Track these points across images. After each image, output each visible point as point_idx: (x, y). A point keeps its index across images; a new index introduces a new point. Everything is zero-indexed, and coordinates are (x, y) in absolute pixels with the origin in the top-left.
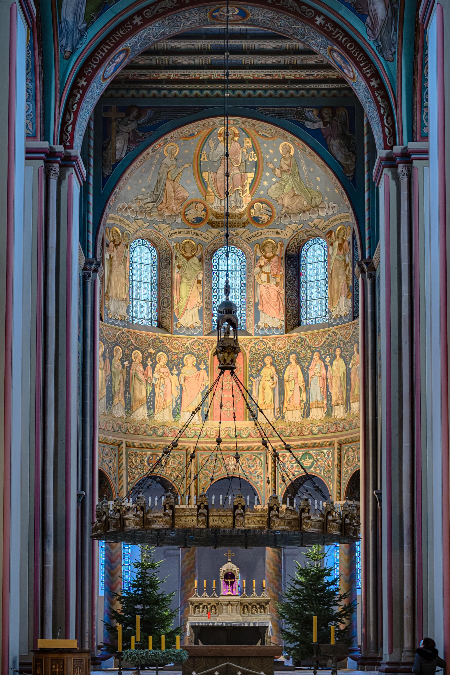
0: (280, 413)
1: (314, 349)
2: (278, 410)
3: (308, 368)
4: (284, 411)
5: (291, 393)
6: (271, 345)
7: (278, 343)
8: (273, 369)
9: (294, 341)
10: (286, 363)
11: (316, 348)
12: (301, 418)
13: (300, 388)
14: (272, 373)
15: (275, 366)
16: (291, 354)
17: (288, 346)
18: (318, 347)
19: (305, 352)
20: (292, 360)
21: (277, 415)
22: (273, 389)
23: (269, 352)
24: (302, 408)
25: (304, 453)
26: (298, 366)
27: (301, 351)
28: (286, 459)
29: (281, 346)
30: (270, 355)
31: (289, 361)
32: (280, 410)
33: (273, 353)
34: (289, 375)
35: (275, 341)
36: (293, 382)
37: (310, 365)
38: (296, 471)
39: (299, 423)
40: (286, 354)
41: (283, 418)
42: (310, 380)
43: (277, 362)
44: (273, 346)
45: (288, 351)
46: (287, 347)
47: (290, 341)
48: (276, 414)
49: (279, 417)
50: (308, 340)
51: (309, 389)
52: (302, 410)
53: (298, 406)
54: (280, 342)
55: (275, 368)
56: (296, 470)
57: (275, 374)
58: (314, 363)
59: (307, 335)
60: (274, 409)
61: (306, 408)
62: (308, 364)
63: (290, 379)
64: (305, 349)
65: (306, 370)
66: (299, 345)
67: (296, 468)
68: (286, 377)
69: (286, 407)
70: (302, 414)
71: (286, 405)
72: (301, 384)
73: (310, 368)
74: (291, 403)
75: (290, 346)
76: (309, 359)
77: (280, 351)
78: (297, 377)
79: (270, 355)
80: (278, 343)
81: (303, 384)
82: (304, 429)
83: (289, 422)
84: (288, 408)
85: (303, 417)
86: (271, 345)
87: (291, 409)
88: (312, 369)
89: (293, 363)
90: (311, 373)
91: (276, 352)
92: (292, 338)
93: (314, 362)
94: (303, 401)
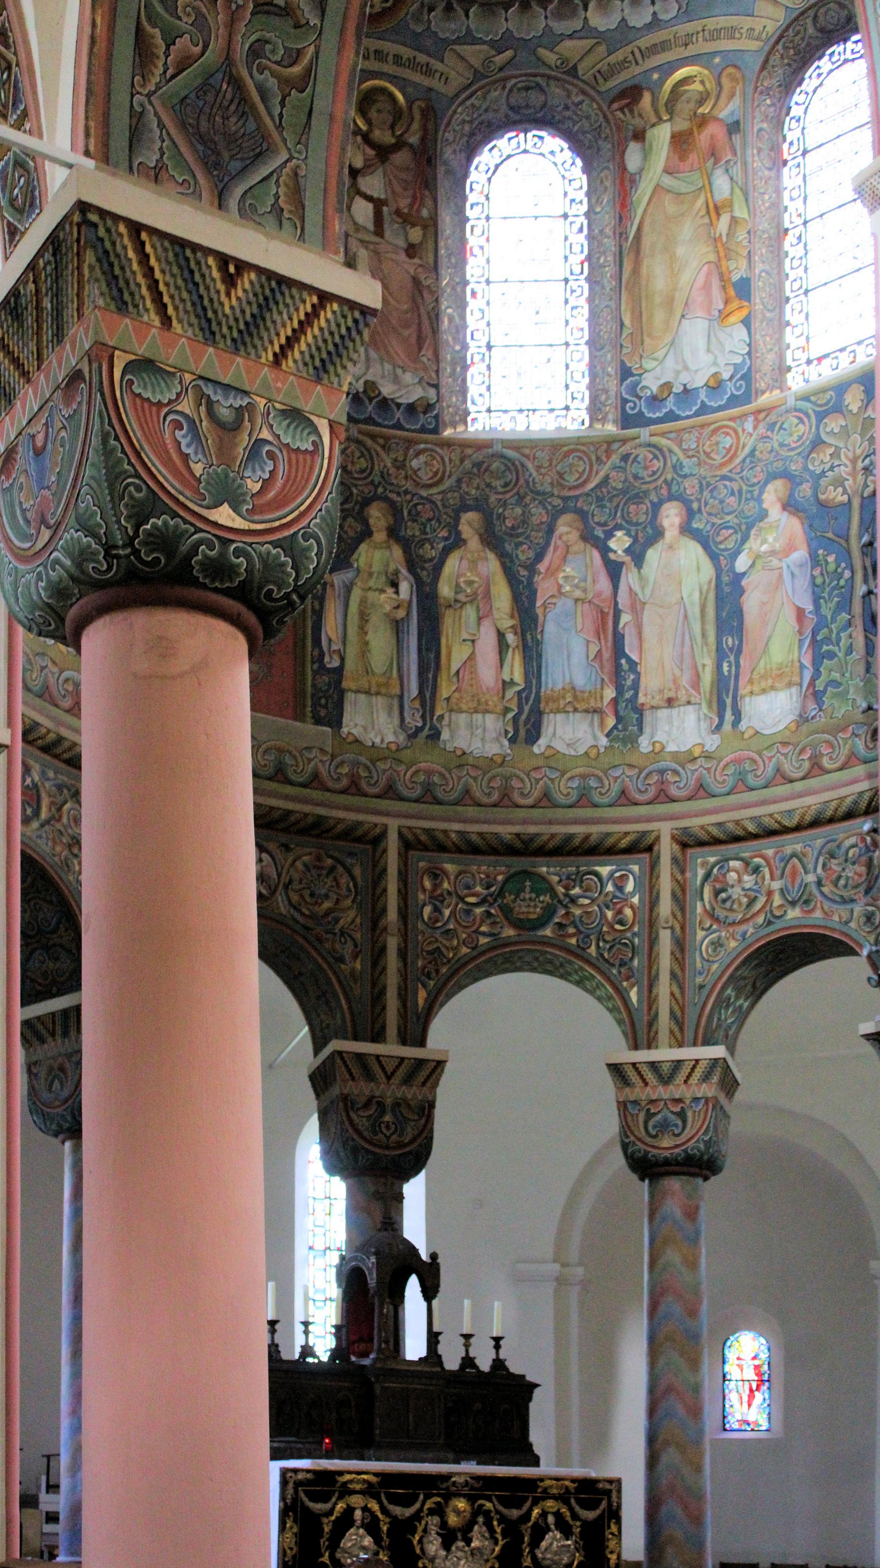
0: (423, 717)
1: (557, 502)
2: (417, 704)
3: (531, 568)
4: (438, 712)
5: (466, 651)
6: (389, 465)
7: (415, 463)
8: (397, 552)
9: (478, 465)
10: (446, 539)
11: (565, 499)
12: (506, 743)
13: (501, 636)
14: (392, 567)
15: (406, 545)
16: (466, 508)
17: (454, 478)
18: (577, 498)
19: (518, 511)
20: (466, 530)
21: (414, 720)
22: (398, 627)
23: (380, 490)
24: (507, 710)
25: (513, 871)
26: (491, 556)
27: (505, 505)
28: (446, 885)
29: (425, 476)
30: (386, 499)
31: (458, 533)
32: (423, 704)
33: (398, 494)
34: (457, 585)
35: (406, 455)
36: (470, 613)
37: (539, 557)
38: (484, 934)
39: (499, 761)
40: (444, 506)
41: (435, 735)
42: (539, 611)
43: (412, 530)
44: (398, 468)
45: (453, 499)
46: (447, 484)
47: (462, 461)
48: (408, 719)
49: (419, 730)
50: (530, 466)
51: (538, 643)
52: (510, 715)
53: (493, 700)
54: (422, 458)
55: (405, 552)
56: (483, 929)
57: (404, 571)
58: (559, 552)
59: (527, 451)
60: (401, 697)
61: (527, 709)
62: (531, 554)
63: (461, 597)
64: (521, 498)
65: (523, 572)
66: (497, 484)
67: (482, 922)
68: (445, 590)
69: (448, 699)
70: (510, 729)
71: (445, 690)
72: (506, 623)
73: (542, 567)
74: (465, 686)
75: (459, 481)
76: (538, 537)
77: (424, 493)
78: (487, 594)
79: (386, 499)
80: (415, 463)
81: (511, 623)
82: (515, 783)
83: (459, 753)
84: (453, 700)
85: (513, 741)
86: (389, 465)
87: (464, 707)
88: (552, 572)
89: (474, 543)
90: (544, 588)
91: (406, 492)
92: (469, 451)
93: (556, 548)
94: (512, 683)
